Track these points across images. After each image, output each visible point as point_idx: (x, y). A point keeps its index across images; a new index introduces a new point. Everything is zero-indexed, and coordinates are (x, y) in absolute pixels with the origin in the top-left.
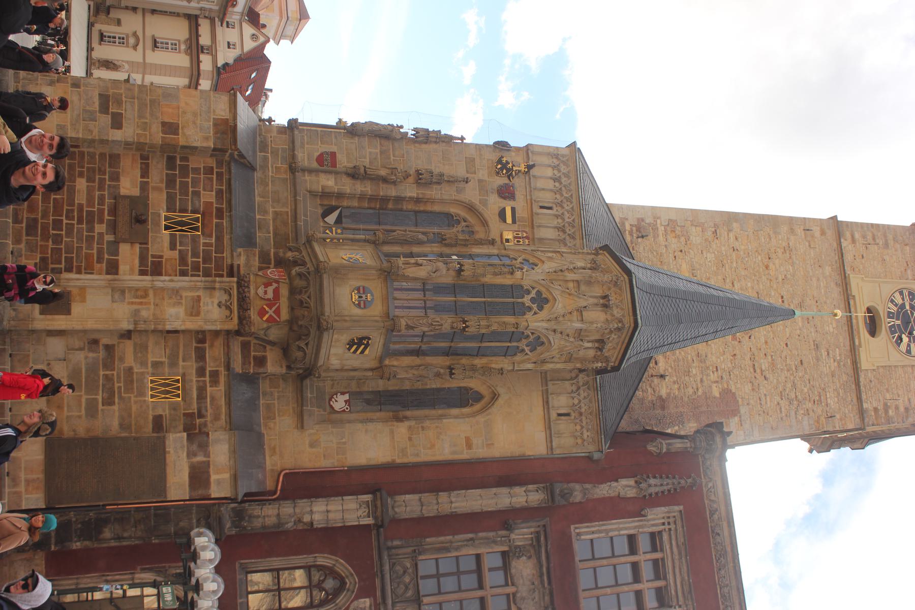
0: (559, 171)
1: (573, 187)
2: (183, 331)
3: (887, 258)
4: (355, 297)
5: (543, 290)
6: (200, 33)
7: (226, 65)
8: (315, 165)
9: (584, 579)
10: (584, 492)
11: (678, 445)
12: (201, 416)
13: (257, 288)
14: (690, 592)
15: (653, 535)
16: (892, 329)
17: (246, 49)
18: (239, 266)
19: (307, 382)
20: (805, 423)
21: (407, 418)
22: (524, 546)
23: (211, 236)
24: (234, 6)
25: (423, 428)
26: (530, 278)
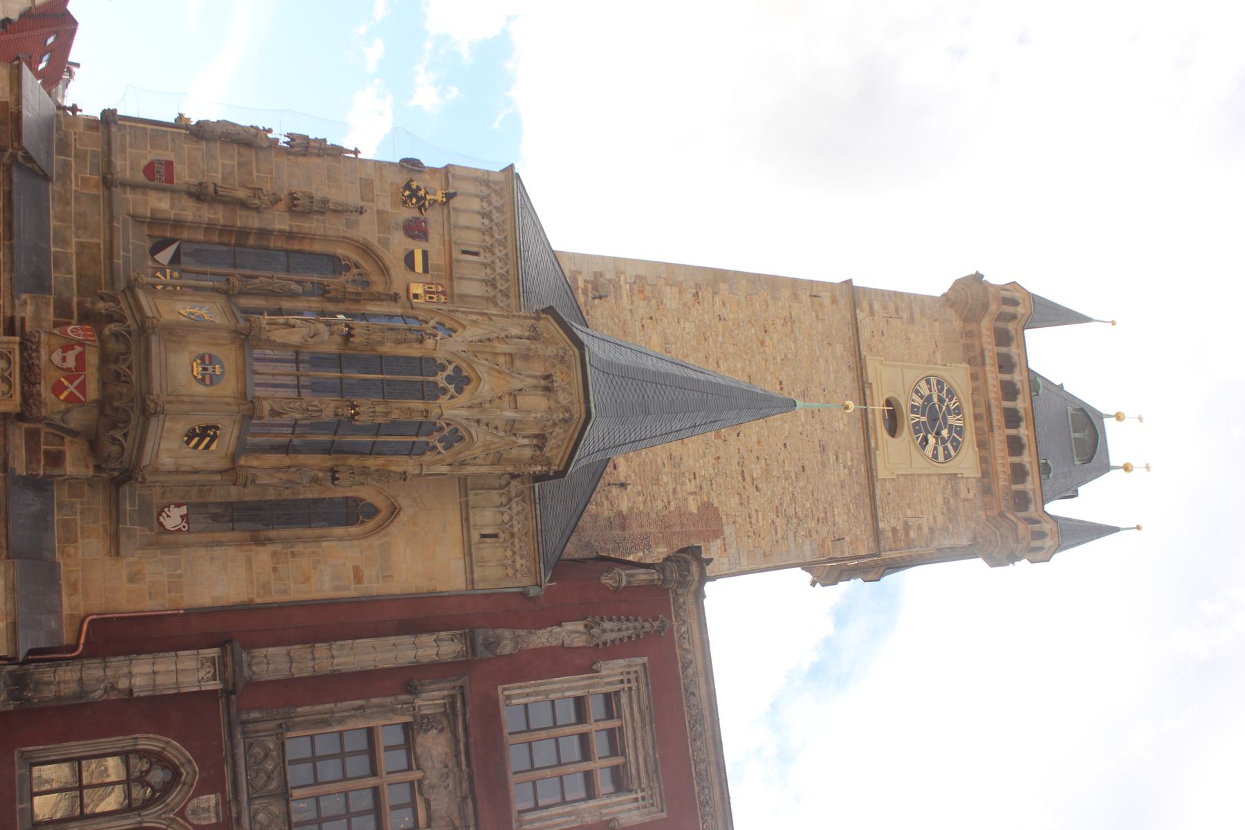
0: (490, 203)
1: (508, 226)
4: (197, 369)
5: (464, 365)
8: (141, 178)
9: (516, 757)
10: (516, 640)
11: (642, 576)
13: (51, 353)
14: (656, 771)
15: (607, 697)
16: (916, 428)
18: (23, 319)
19: (126, 489)
20: (807, 547)
21: (270, 540)
22: (434, 716)
25: (293, 554)
26: (445, 348)
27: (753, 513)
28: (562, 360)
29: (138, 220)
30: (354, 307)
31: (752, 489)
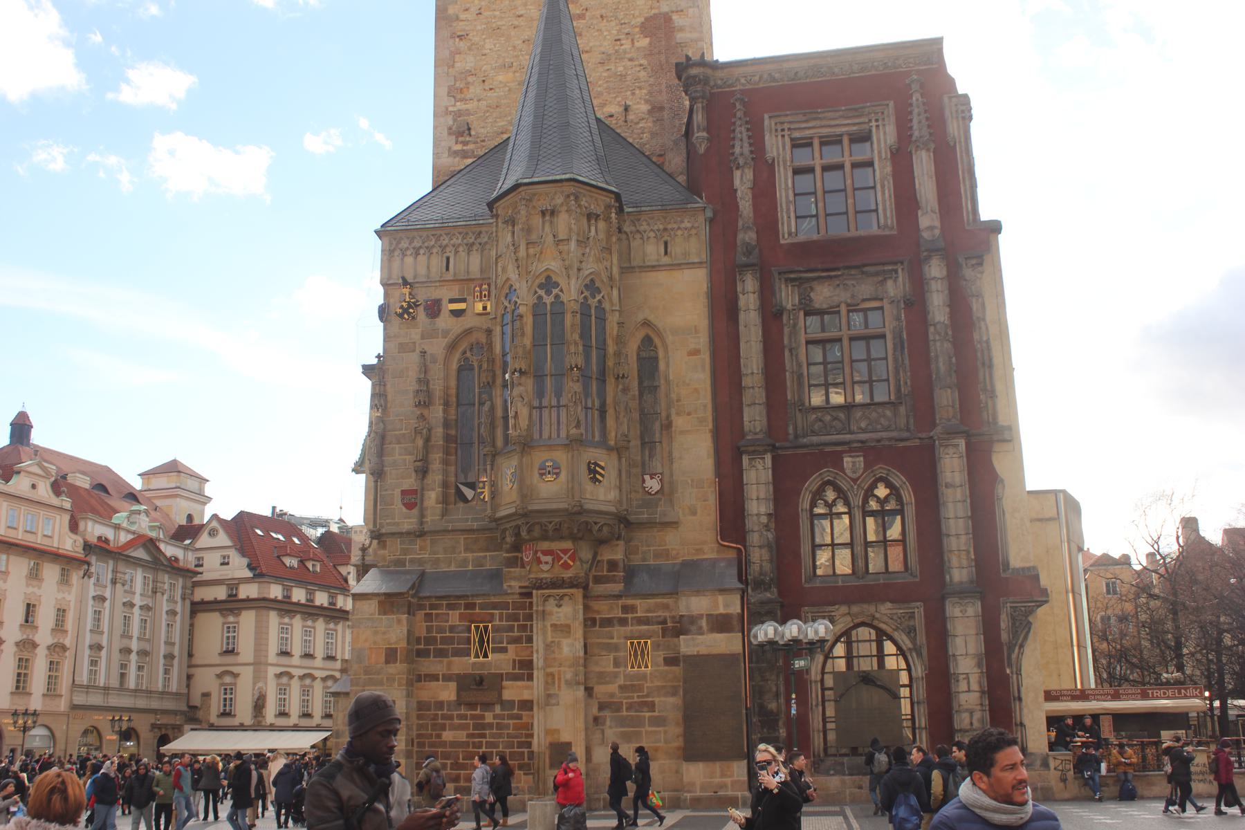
0: (407, 249)
1: (424, 234)
2: (585, 639)
4: (549, 478)
5: (537, 282)
6: (212, 599)
8: (415, 511)
9: (837, 229)
11: (699, 118)
15: (794, 146)
17: (229, 543)
19: (632, 518)
21: (668, 417)
23: (492, 615)
24: (177, 559)
26: (525, 296)
28: (530, 200)
29: (445, 513)
30: (498, 363)
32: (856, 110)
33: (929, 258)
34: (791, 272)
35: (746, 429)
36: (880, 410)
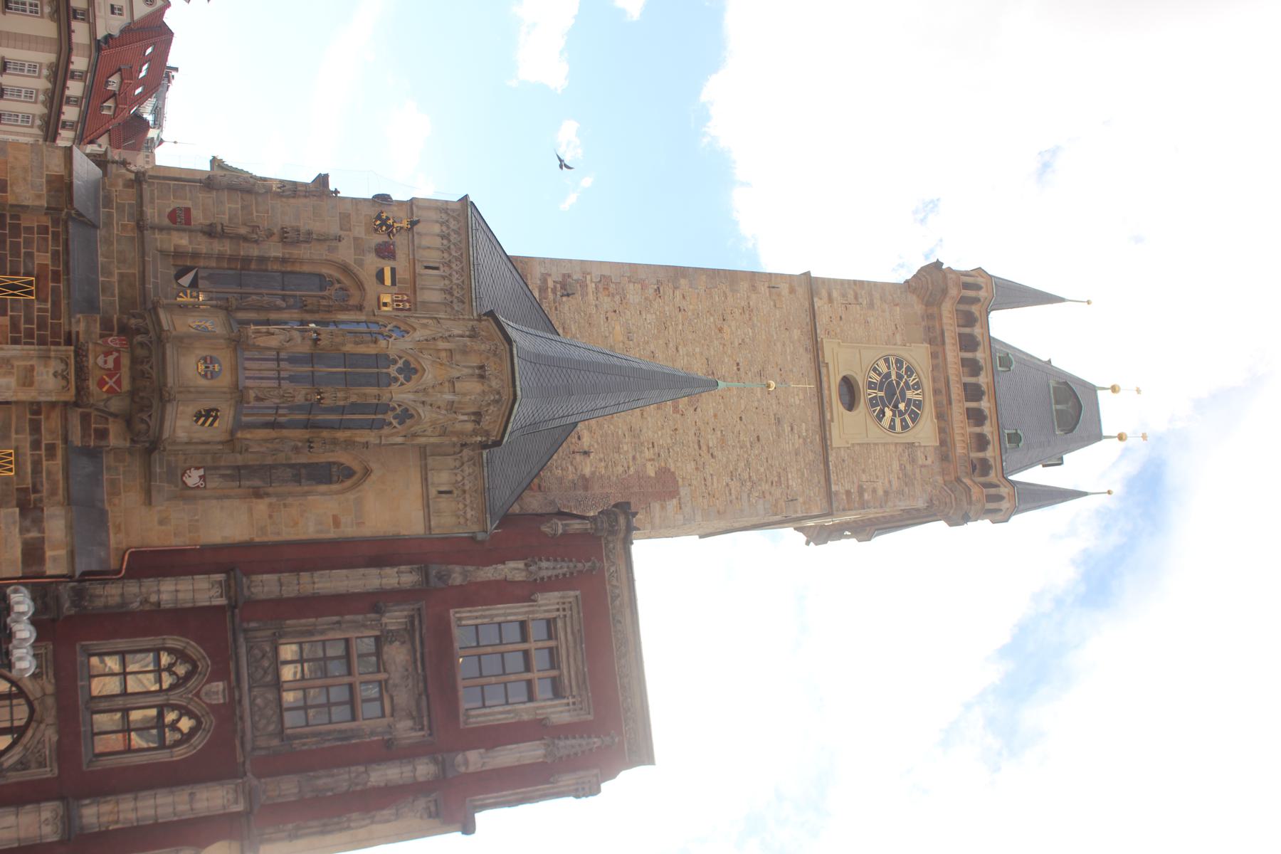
0: (448, 227)
1: (463, 245)
2: (16, 403)
3: (871, 320)
4: (201, 367)
5: (411, 360)
7: (109, 37)
8: (166, 222)
11: (576, 525)
12: (35, 490)
13: (96, 358)
16: (873, 402)
17: (137, 16)
18: (78, 333)
19: (156, 455)
21: (268, 495)
22: (397, 631)
23: (46, 301)
25: (285, 505)
26: (397, 346)
27: (709, 477)
28: (495, 354)
29: (164, 254)
30: (327, 317)
31: (708, 457)
32: (584, 682)
33: (436, 762)
34: (420, 621)
35: (254, 577)
36: (275, 718)
